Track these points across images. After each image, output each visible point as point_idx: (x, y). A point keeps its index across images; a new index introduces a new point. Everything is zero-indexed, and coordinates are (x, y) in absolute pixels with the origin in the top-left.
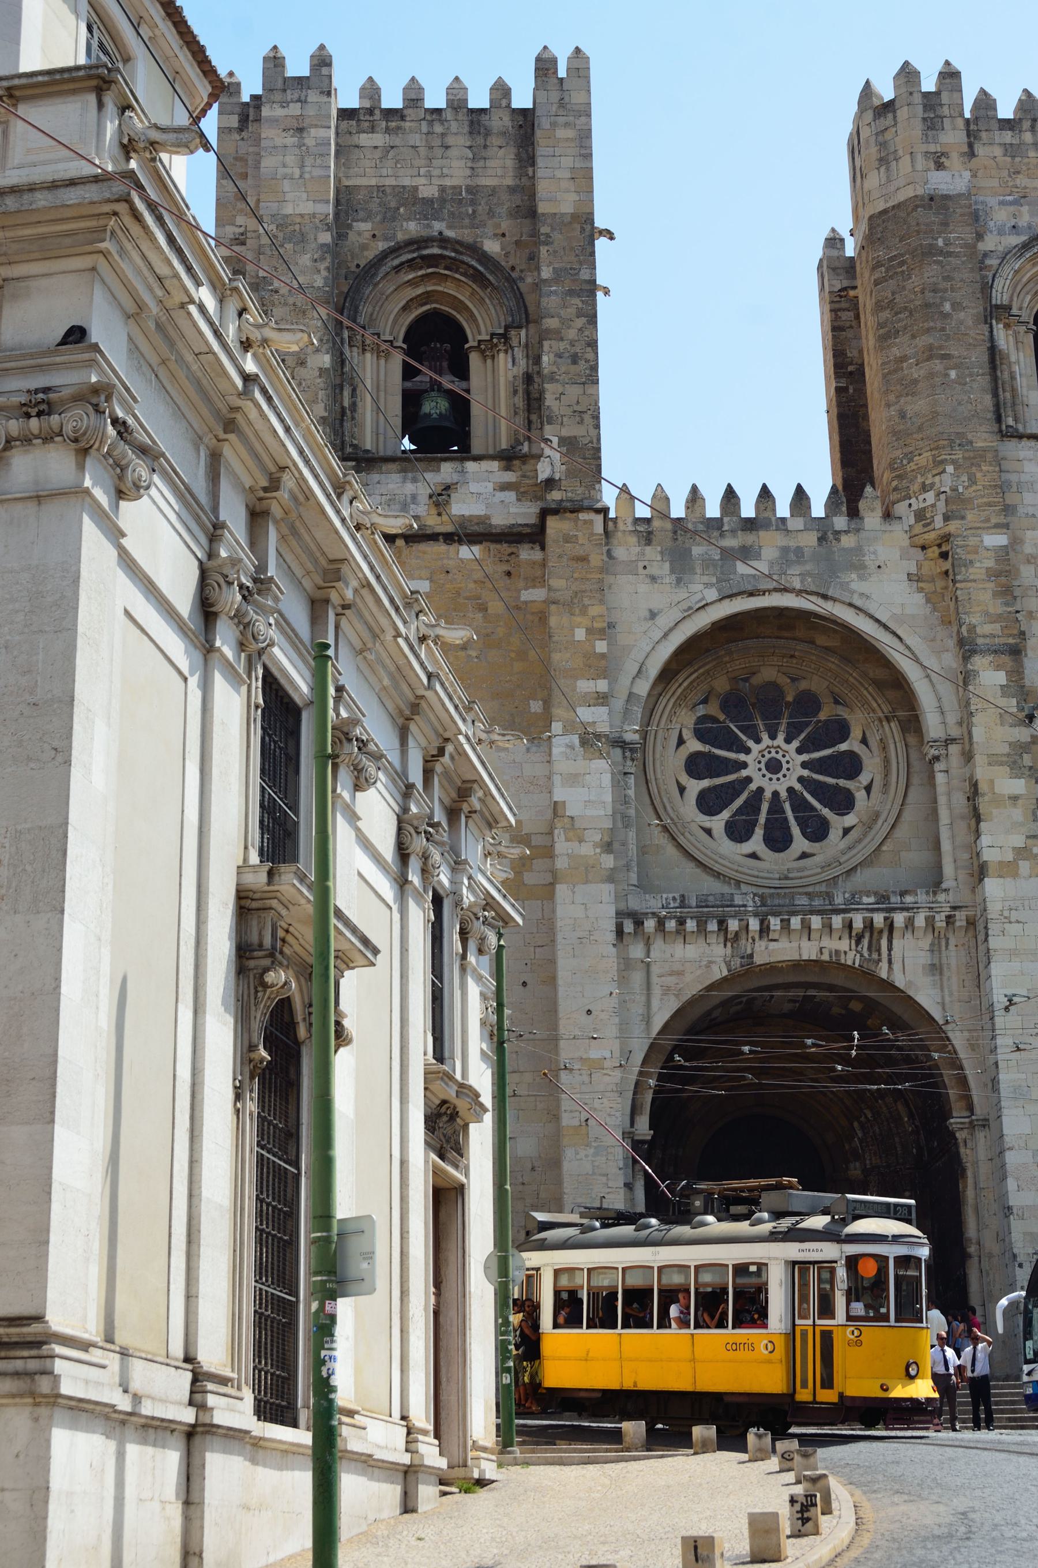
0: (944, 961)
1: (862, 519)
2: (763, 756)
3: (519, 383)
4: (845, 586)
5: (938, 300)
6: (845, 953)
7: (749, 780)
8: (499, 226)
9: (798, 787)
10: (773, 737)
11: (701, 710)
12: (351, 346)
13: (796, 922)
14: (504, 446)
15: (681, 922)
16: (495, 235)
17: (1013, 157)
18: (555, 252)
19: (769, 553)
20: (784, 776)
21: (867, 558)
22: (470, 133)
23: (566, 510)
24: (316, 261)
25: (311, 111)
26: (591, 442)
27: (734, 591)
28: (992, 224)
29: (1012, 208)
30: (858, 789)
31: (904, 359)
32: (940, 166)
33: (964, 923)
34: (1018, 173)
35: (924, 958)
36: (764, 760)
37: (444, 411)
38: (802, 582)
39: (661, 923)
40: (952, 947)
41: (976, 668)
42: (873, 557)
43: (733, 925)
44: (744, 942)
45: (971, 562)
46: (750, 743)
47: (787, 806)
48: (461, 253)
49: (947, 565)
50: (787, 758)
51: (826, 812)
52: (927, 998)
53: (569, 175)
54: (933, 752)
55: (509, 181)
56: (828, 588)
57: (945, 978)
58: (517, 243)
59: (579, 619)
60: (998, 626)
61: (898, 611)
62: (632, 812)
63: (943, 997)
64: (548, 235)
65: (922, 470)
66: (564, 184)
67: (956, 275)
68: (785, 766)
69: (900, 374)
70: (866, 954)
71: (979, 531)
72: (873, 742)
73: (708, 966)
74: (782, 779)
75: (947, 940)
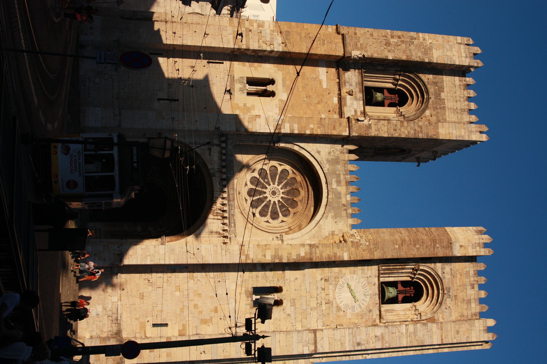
0: (214, 236)
1: (351, 218)
2: (277, 190)
3: (388, 118)
4: (329, 211)
5: (419, 243)
7: (270, 185)
8: (434, 115)
9: (268, 200)
10: (283, 193)
11: (290, 172)
12: (395, 70)
14: (368, 113)
15: (225, 155)
16: (431, 114)
17: (466, 274)
18: (427, 126)
19: (339, 189)
20: (271, 196)
21: (339, 219)
22: (461, 109)
23: (349, 124)
24: (419, 57)
25: (463, 59)
26: (370, 133)
27: (327, 178)
28: (445, 266)
29: (450, 272)
30: (267, 218)
31: (401, 233)
34: (461, 275)
35: (215, 230)
36: (275, 190)
37: (378, 99)
38: (331, 198)
39: (224, 148)
40: (219, 238)
41: (305, 246)
42: (339, 220)
43: (224, 170)
45: (339, 248)
46: (281, 186)
47: (261, 196)
48: (425, 104)
49: (338, 242)
51: (260, 208)
53: (450, 132)
54: (279, 236)
55: (448, 119)
56: (329, 206)
58: (429, 120)
59: (316, 126)
60: (319, 255)
61: (323, 227)
64: (432, 124)
65: (367, 237)
66: (447, 131)
67: (428, 249)
68: (274, 197)
69: (396, 232)
70: (215, 211)
71: (348, 251)
72: (283, 224)
74: (270, 195)
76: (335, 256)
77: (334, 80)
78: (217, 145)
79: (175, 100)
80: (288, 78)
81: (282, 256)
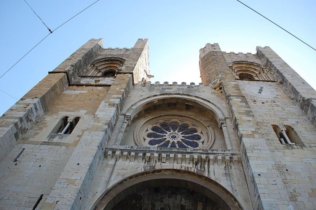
0: (230, 172)
6: (191, 168)
7: (166, 139)
9: (181, 141)
11: (154, 125)
13: (172, 155)
20: (177, 139)
30: (199, 142)
32: (214, 49)
33: (237, 159)
36: (171, 136)
39: (122, 153)
43: (148, 155)
44: (152, 162)
47: (177, 145)
50: (178, 135)
52: (224, 183)
57: (231, 178)
62: (123, 130)
63: (231, 184)
68: (177, 137)
73: (137, 168)
75: (231, 166)
76: (236, 87)
77: (84, 87)
78: (116, 161)
79: (41, 198)
80: (67, 109)
81: (245, 111)
